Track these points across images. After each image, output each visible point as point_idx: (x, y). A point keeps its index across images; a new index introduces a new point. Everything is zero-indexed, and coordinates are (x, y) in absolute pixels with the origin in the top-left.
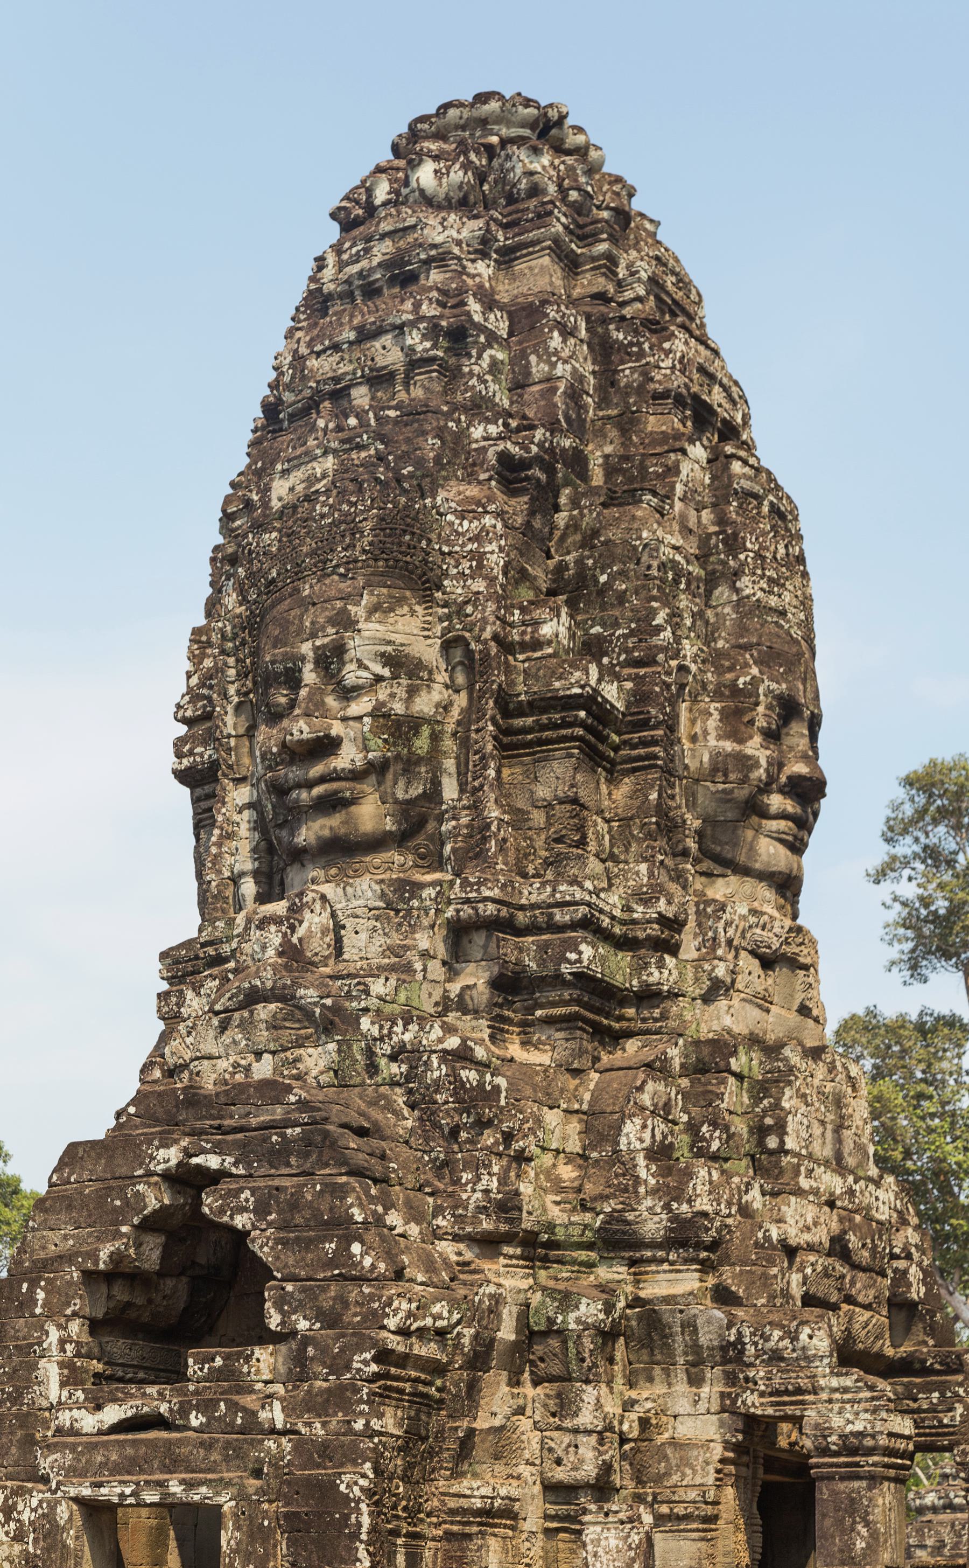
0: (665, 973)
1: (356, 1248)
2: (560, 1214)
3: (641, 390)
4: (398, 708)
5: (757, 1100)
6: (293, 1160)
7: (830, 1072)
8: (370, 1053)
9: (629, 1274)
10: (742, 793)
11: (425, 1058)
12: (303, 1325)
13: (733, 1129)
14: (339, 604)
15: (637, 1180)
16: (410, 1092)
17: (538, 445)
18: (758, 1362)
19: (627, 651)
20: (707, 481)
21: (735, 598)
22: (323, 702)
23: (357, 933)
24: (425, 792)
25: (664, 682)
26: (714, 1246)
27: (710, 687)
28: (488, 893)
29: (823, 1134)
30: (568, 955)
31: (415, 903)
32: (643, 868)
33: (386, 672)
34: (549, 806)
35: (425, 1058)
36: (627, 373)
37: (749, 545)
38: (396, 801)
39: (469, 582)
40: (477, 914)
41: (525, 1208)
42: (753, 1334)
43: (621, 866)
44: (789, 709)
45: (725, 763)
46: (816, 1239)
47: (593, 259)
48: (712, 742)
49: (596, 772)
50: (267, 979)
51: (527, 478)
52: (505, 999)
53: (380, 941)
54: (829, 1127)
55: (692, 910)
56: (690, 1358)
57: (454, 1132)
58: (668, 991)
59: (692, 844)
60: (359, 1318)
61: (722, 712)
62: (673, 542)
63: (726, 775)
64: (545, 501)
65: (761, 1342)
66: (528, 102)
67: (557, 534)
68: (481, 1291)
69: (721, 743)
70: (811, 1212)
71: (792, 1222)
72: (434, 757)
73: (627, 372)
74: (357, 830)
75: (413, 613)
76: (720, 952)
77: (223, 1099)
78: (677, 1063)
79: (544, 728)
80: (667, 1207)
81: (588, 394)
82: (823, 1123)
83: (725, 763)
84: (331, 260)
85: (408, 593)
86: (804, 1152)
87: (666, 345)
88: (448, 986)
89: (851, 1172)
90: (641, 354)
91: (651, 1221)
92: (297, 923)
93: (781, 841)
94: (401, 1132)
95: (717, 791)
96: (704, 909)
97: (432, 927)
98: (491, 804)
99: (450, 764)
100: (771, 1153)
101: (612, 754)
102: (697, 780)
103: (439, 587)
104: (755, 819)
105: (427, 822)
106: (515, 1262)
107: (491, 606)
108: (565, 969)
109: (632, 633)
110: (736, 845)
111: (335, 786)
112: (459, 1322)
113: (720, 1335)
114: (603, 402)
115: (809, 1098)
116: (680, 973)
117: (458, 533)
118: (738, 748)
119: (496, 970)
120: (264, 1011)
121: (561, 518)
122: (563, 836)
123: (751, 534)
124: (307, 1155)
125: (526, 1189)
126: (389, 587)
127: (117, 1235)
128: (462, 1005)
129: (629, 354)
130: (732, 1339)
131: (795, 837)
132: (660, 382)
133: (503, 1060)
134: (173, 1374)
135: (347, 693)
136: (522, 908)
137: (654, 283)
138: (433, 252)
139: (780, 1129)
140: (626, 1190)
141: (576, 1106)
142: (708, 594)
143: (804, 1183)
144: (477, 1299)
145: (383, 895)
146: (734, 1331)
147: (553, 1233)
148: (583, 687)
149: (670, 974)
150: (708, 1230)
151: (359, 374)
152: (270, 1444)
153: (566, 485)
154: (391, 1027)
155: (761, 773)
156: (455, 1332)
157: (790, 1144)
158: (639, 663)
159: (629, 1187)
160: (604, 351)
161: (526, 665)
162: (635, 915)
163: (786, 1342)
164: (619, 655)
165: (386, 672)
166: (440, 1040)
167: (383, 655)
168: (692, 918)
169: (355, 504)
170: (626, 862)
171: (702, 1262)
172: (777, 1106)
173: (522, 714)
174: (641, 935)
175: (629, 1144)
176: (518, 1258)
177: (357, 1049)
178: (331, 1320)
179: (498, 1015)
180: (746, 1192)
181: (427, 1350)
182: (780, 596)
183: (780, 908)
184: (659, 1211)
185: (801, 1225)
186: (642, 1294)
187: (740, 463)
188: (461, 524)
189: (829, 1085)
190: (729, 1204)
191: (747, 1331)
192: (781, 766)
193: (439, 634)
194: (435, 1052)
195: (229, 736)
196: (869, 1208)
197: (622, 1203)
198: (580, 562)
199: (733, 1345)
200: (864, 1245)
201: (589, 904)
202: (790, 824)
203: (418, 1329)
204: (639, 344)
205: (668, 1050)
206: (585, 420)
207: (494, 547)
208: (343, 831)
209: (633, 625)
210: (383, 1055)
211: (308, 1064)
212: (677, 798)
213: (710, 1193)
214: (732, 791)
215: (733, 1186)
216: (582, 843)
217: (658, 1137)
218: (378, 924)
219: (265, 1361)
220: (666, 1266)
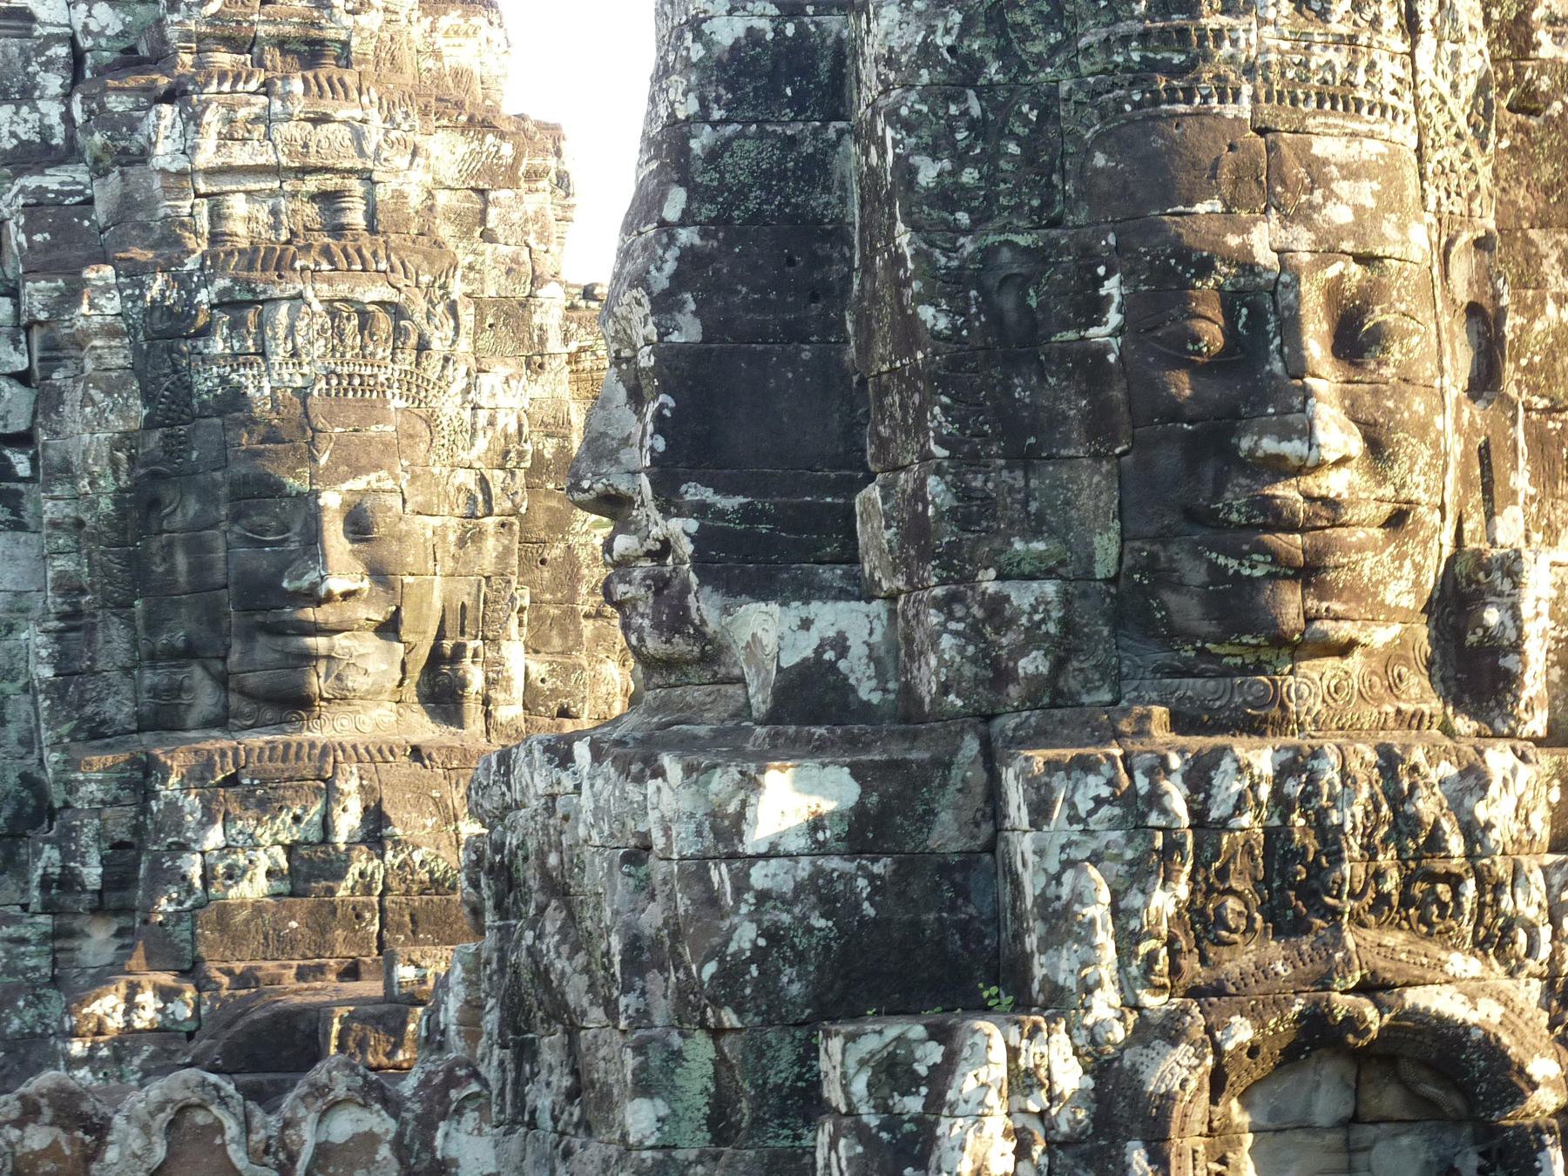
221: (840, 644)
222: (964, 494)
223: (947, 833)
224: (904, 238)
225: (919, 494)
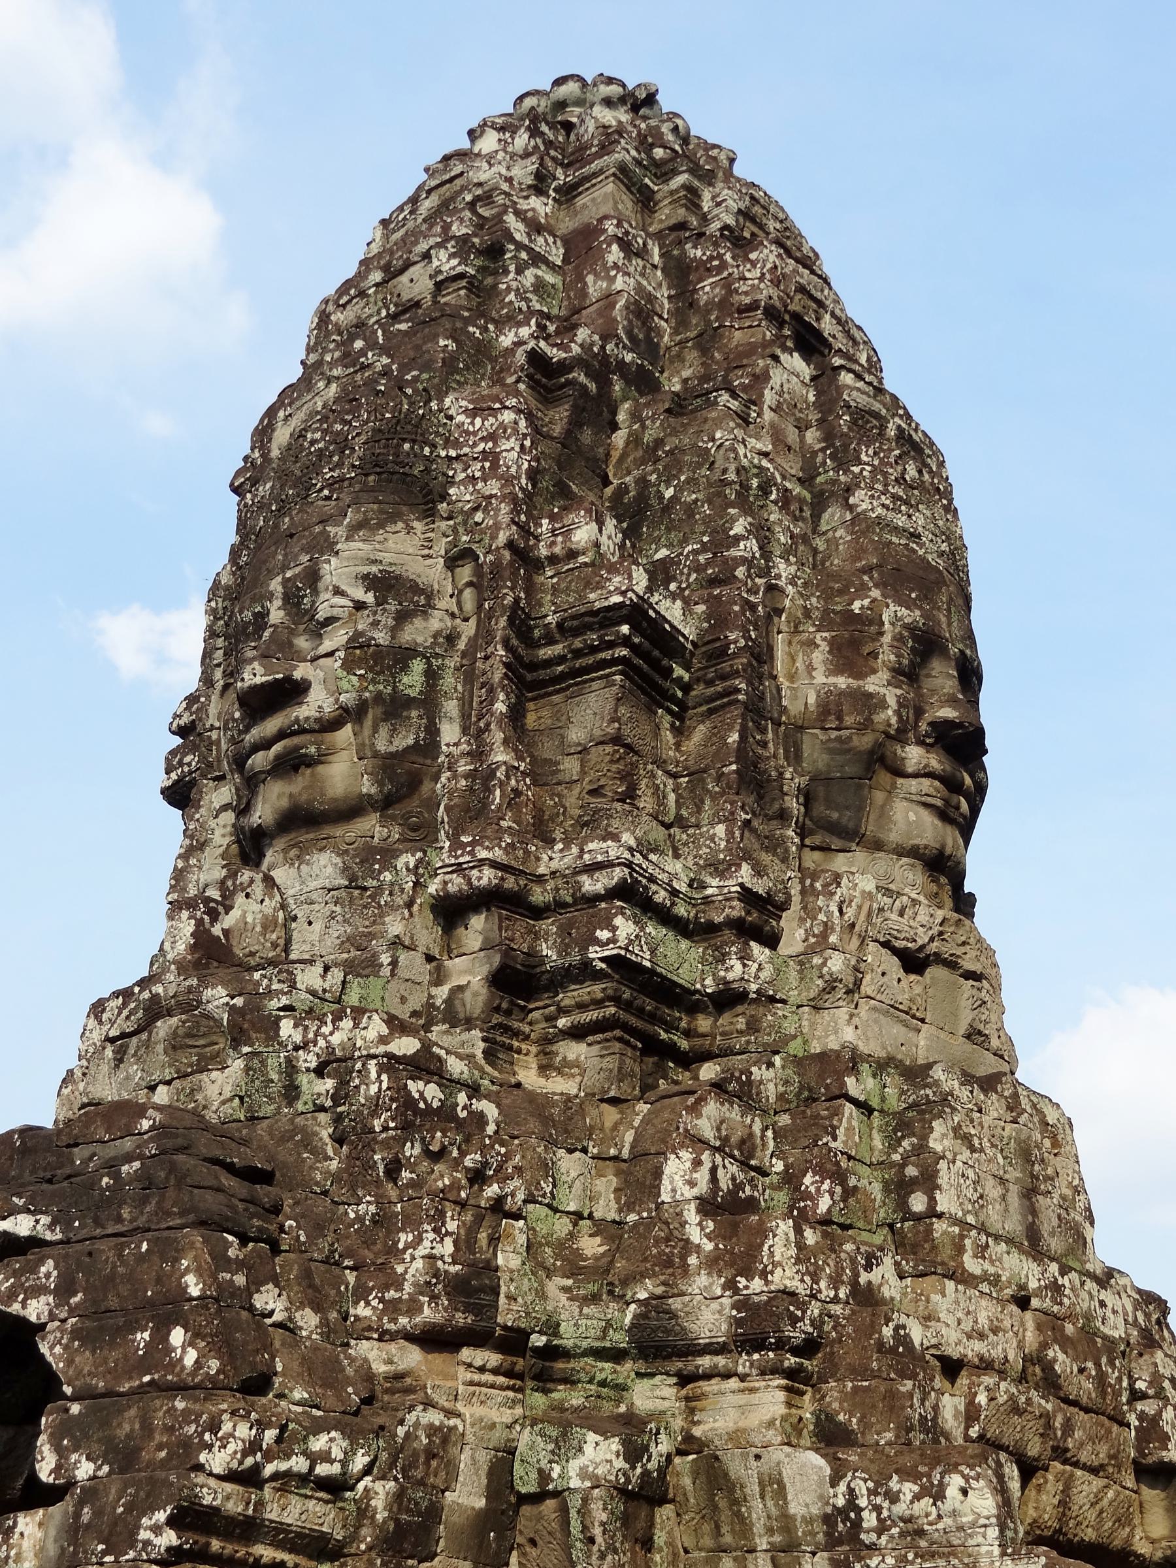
0: (749, 967)
2: (567, 1303)
3: (724, 305)
4: (381, 637)
5: (893, 1143)
6: (126, 1213)
7: (1010, 1109)
8: (291, 1068)
9: (678, 1399)
10: (865, 741)
11: (358, 1066)
13: (852, 1181)
14: (317, 529)
15: (687, 1247)
16: (338, 1119)
17: (581, 346)
18: (884, 1539)
19: (699, 568)
20: (812, 398)
21: (848, 517)
22: (290, 644)
23: (310, 923)
24: (417, 742)
25: (747, 602)
26: (809, 1347)
27: (816, 614)
28: (483, 854)
29: (1003, 1198)
30: (598, 933)
31: (387, 876)
32: (720, 830)
33: (370, 598)
34: (584, 751)
35: (358, 1066)
36: (707, 289)
37: (864, 458)
38: (376, 755)
39: (480, 485)
40: (470, 883)
41: (503, 1289)
42: (872, 1493)
43: (691, 831)
44: (925, 645)
45: (839, 704)
46: (996, 1353)
47: (672, 193)
48: (820, 678)
49: (656, 713)
51: (569, 383)
52: (512, 1003)
53: (338, 930)
54: (1014, 1189)
55: (795, 890)
56: (777, 1538)
57: (393, 1171)
58: (758, 992)
59: (794, 805)
60: (163, 1454)
61: (832, 643)
62: (759, 446)
63: (840, 718)
64: (596, 413)
65: (886, 1504)
67: (615, 455)
68: (411, 1418)
69: (832, 680)
70: (985, 1312)
71: (951, 1320)
72: (429, 702)
73: (707, 289)
74: (323, 794)
75: (409, 529)
76: (833, 939)
77: (65, 1140)
78: (771, 1091)
79: (578, 654)
80: (731, 1285)
81: (661, 317)
82: (1002, 1181)
83: (839, 704)
85: (404, 508)
86: (970, 1219)
87: (753, 256)
88: (434, 991)
89: (1052, 1259)
90: (723, 265)
91: (708, 1312)
92: (221, 909)
93: (925, 805)
94: (318, 1177)
95: (830, 740)
96: (812, 885)
97: (409, 905)
98: (498, 747)
99: (451, 707)
100: (918, 1218)
101: (679, 694)
102: (802, 727)
103: (444, 497)
104: (884, 777)
105: (421, 782)
106: (488, 1377)
107: (505, 508)
108: (594, 953)
109: (704, 548)
110: (860, 809)
111: (296, 740)
112: (367, 1470)
113: (821, 1497)
114: (680, 320)
115: (976, 1142)
116: (778, 971)
117: (468, 433)
118: (854, 683)
119: (497, 960)
121: (619, 438)
122: (602, 787)
123: (868, 447)
124: (145, 1201)
125: (508, 1259)
126: (380, 503)
129: (708, 270)
130: (841, 1502)
131: (946, 801)
132: (746, 293)
133: (501, 1085)
135: (318, 629)
136: (540, 879)
138: (479, 192)
139: (928, 1182)
140: (669, 1263)
141: (613, 1152)
142: (816, 517)
143: (972, 1265)
144: (401, 1431)
145: (345, 869)
146: (842, 1487)
147: (556, 1334)
148: (624, 593)
149: (760, 969)
150: (794, 1320)
151: (384, 313)
153: (625, 399)
154: (319, 1027)
155: (889, 716)
156: (361, 1486)
157: (944, 1203)
158: (714, 582)
159: (672, 1260)
160: (682, 274)
161: (555, 580)
162: (709, 891)
163: (927, 1501)
164: (689, 575)
165: (370, 598)
166: (383, 1040)
167: (365, 577)
168: (796, 899)
169: (350, 423)
170: (698, 826)
171: (792, 1374)
172: (921, 1148)
173: (551, 642)
174: (718, 919)
175: (674, 1190)
176: (495, 1372)
177: (274, 1064)
178: (123, 1458)
179: (500, 1025)
180: (868, 1267)
182: (910, 516)
184: (719, 1292)
185: (967, 1326)
186: (697, 1432)
187: (851, 375)
188: (472, 423)
189: (1009, 1127)
190: (835, 1282)
191: (861, 1487)
192: (919, 712)
193: (443, 552)
194: (374, 1057)
195: (212, 728)
196: (1089, 1317)
197: (664, 1284)
198: (642, 482)
199: (841, 1512)
200: (1081, 1371)
201: (629, 865)
202: (937, 783)
203: (276, 1476)
204: (720, 257)
205: (754, 1069)
206: (658, 345)
207: (512, 443)
208: (304, 797)
209: (706, 539)
210: (308, 1070)
211: (209, 1093)
212: (771, 745)
213: (798, 1261)
214: (849, 738)
215: (843, 1255)
216: (629, 796)
217: (725, 1183)
218: (338, 909)
220: (733, 1383)
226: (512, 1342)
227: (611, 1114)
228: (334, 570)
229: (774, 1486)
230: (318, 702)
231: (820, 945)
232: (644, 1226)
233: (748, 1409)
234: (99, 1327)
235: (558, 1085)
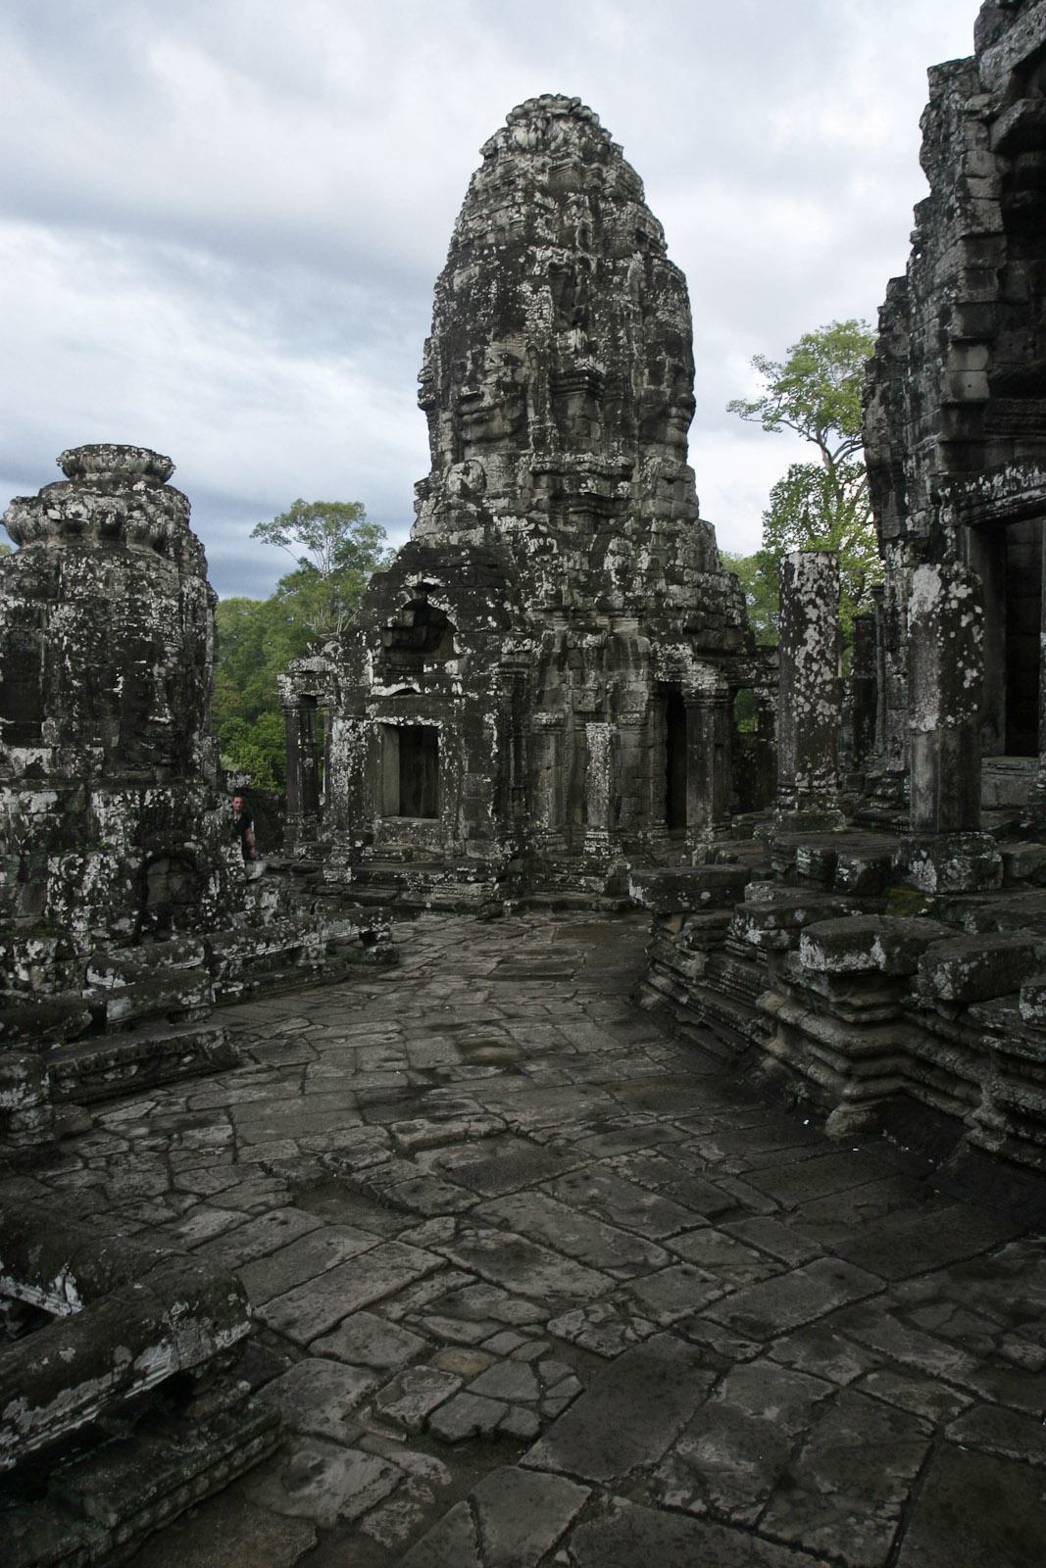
1: (490, 619)
4: (507, 379)
10: (658, 409)
12: (469, 651)
15: (612, 583)
36: (607, 223)
50: (454, 500)
59: (636, 432)
66: (564, 98)
84: (478, 176)
91: (617, 599)
99: (531, 402)
120: (454, 513)
127: (394, 613)
128: (537, 508)
134: (418, 673)
135: (486, 373)
137: (620, 177)
152: (456, 701)
181: (521, 659)
183: (677, 457)
216: (589, 434)
219: (452, 666)
221: (40, 759)
222: (81, 726)
223: (75, 806)
224: (68, 663)
225: (69, 724)
226: (565, 609)
227: (586, 538)
228: (491, 351)
229: (634, 644)
230: (488, 401)
231: (644, 481)
232: (598, 575)
233: (629, 626)
234: (461, 614)
235: (572, 529)
